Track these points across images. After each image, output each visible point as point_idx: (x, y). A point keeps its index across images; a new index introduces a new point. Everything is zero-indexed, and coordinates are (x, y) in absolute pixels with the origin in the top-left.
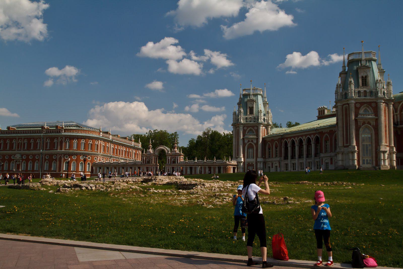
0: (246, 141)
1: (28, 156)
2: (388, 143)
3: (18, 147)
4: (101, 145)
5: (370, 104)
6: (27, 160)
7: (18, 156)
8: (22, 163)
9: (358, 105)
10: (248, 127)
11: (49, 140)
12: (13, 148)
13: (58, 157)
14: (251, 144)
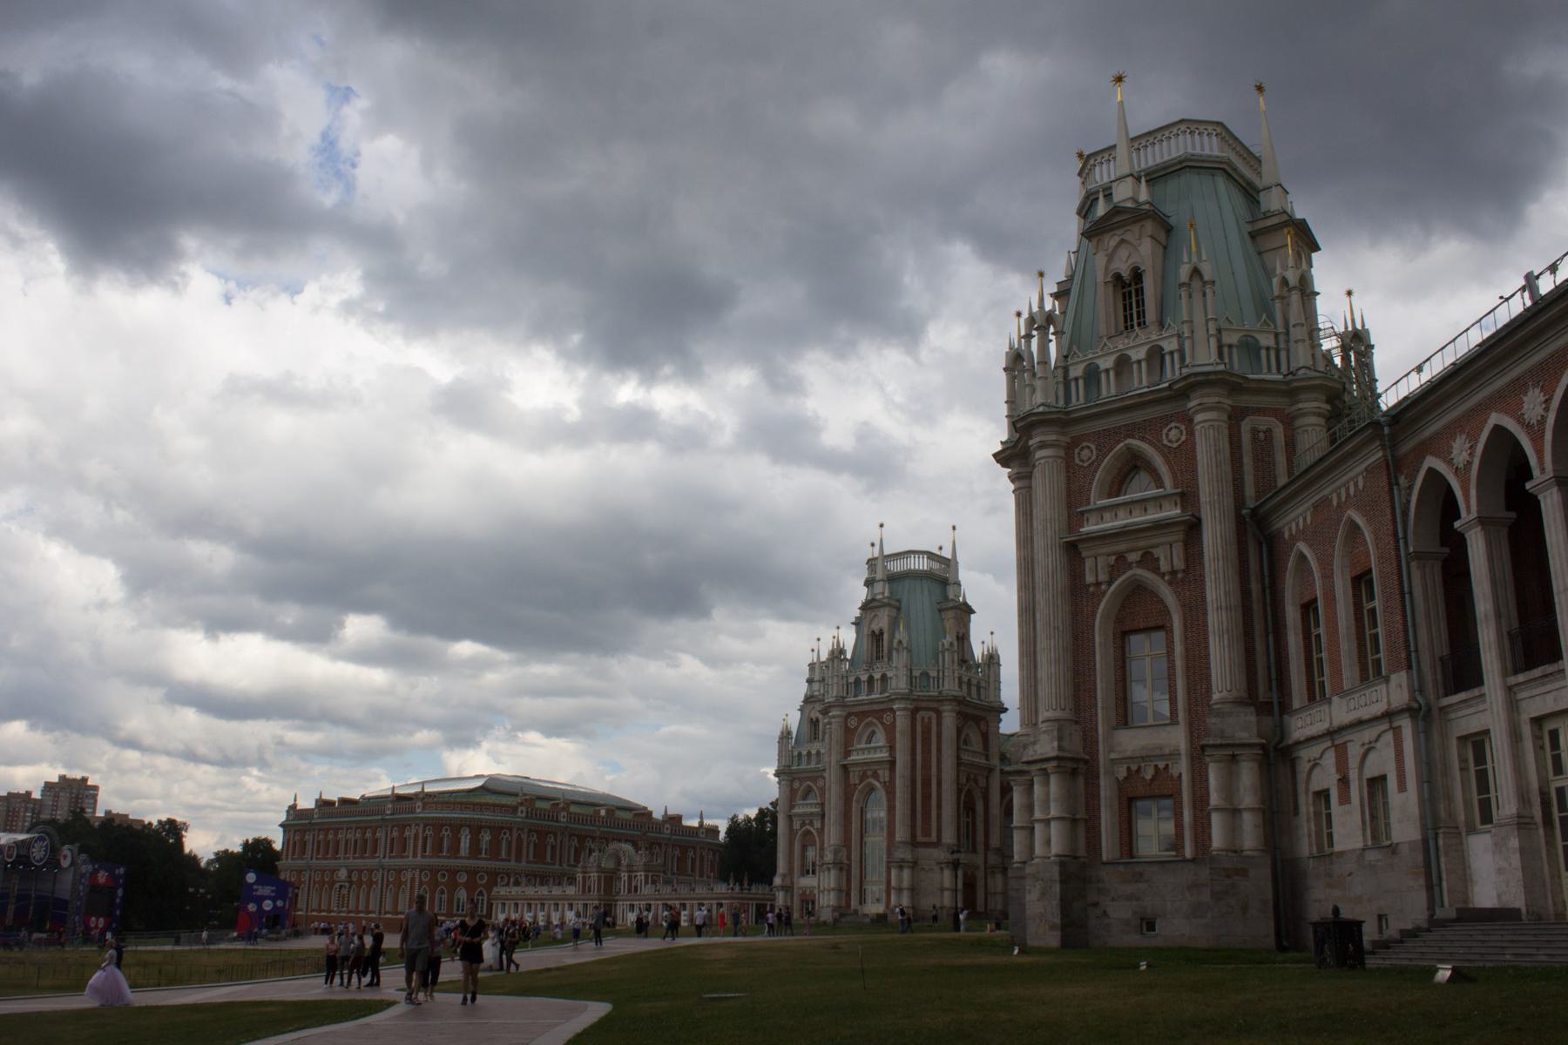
0: (796, 825)
1: (360, 872)
2: (934, 834)
4: (519, 839)
5: (878, 714)
6: (360, 883)
7: (343, 874)
9: (853, 722)
10: (801, 780)
13: (409, 875)
14: (808, 832)
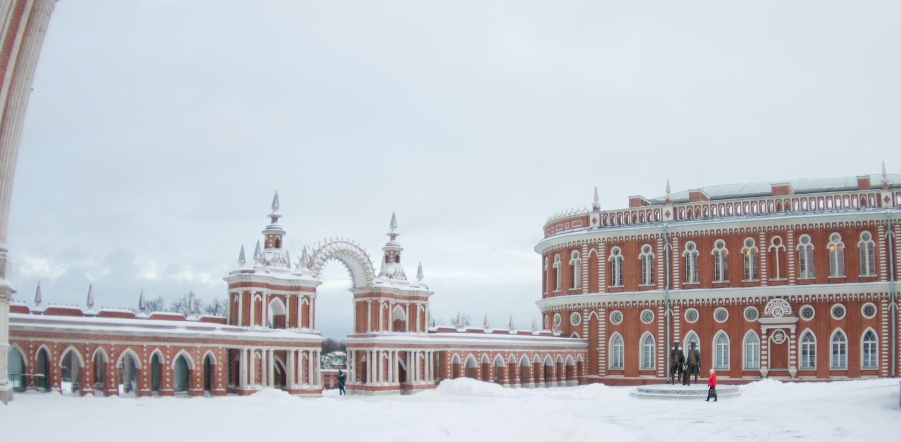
3: (771, 273)
8: (797, 339)
11: (616, 253)
12: (573, 286)
